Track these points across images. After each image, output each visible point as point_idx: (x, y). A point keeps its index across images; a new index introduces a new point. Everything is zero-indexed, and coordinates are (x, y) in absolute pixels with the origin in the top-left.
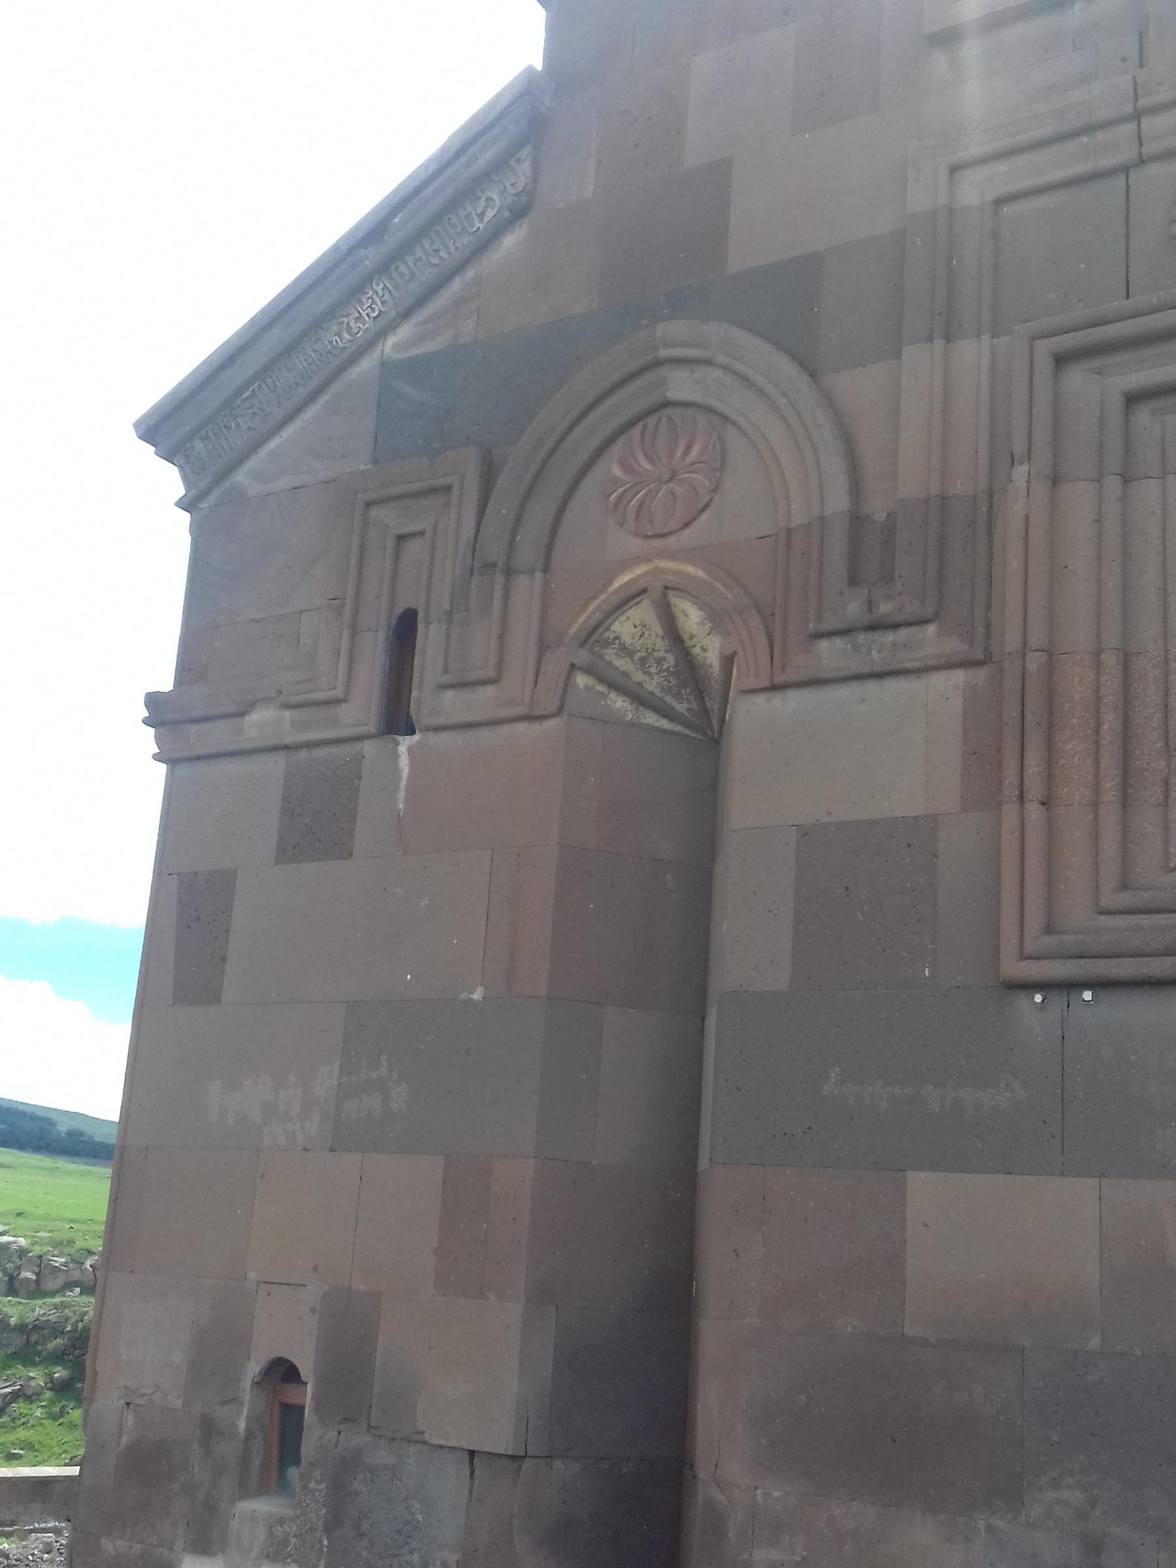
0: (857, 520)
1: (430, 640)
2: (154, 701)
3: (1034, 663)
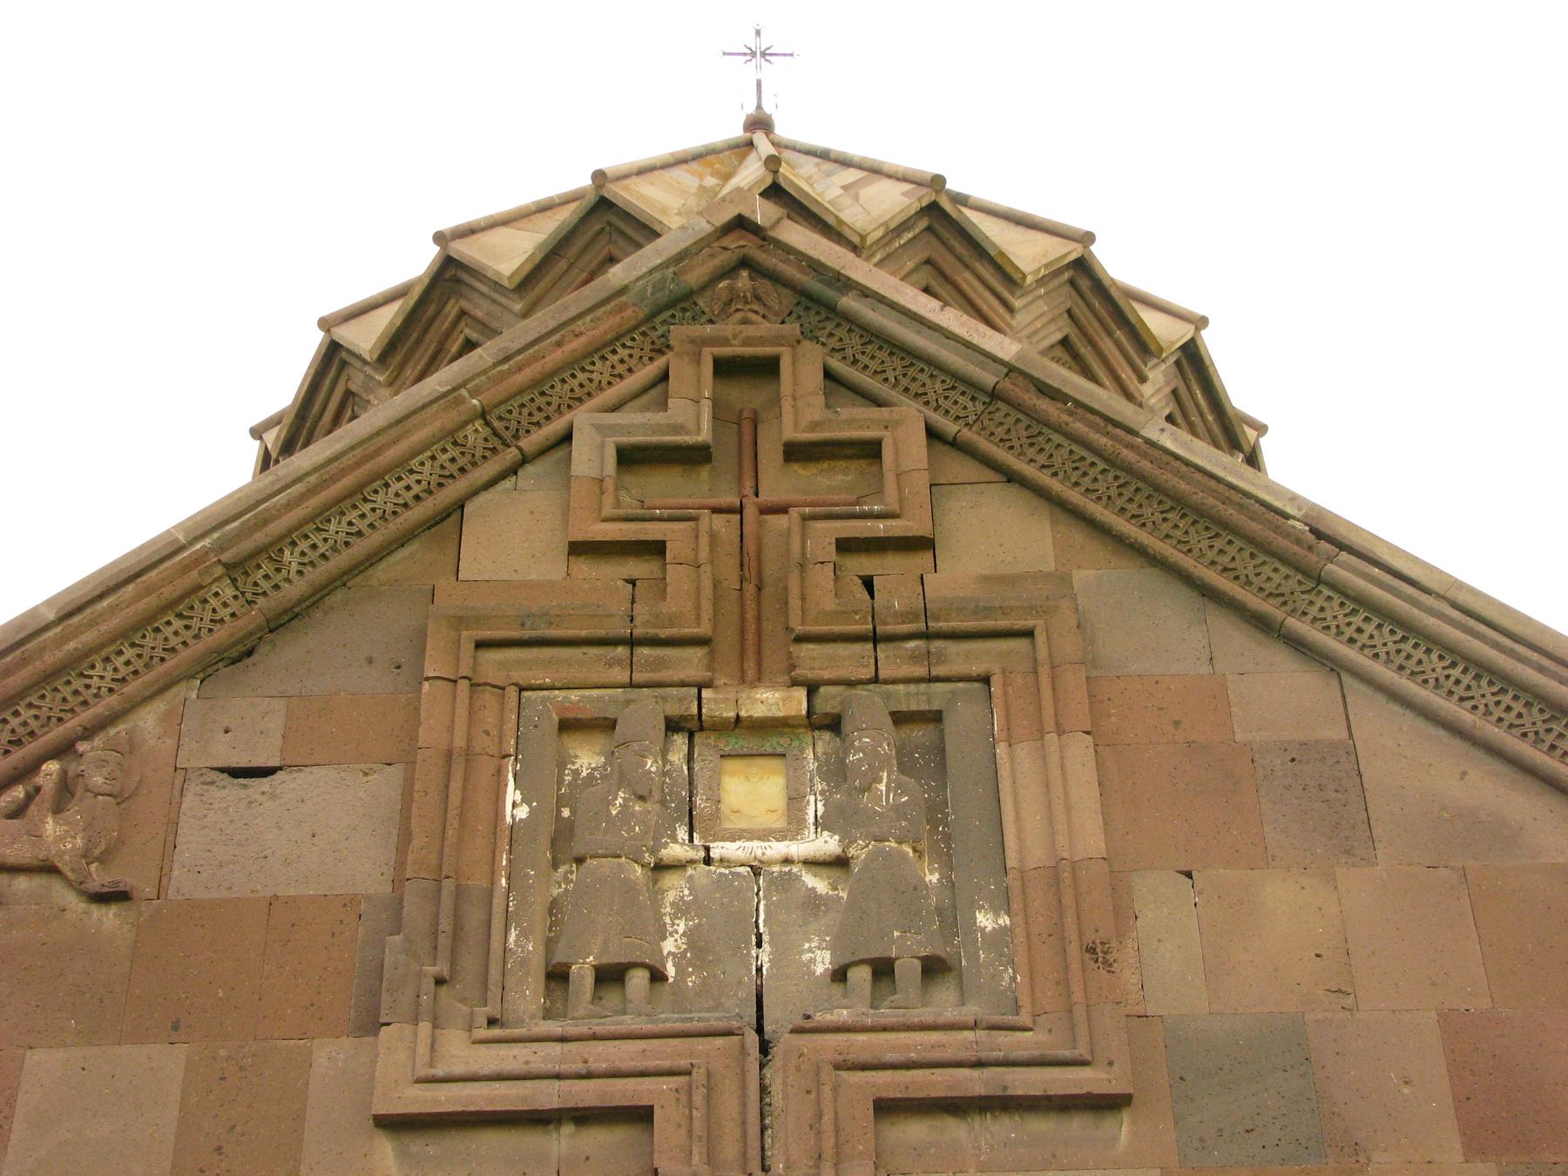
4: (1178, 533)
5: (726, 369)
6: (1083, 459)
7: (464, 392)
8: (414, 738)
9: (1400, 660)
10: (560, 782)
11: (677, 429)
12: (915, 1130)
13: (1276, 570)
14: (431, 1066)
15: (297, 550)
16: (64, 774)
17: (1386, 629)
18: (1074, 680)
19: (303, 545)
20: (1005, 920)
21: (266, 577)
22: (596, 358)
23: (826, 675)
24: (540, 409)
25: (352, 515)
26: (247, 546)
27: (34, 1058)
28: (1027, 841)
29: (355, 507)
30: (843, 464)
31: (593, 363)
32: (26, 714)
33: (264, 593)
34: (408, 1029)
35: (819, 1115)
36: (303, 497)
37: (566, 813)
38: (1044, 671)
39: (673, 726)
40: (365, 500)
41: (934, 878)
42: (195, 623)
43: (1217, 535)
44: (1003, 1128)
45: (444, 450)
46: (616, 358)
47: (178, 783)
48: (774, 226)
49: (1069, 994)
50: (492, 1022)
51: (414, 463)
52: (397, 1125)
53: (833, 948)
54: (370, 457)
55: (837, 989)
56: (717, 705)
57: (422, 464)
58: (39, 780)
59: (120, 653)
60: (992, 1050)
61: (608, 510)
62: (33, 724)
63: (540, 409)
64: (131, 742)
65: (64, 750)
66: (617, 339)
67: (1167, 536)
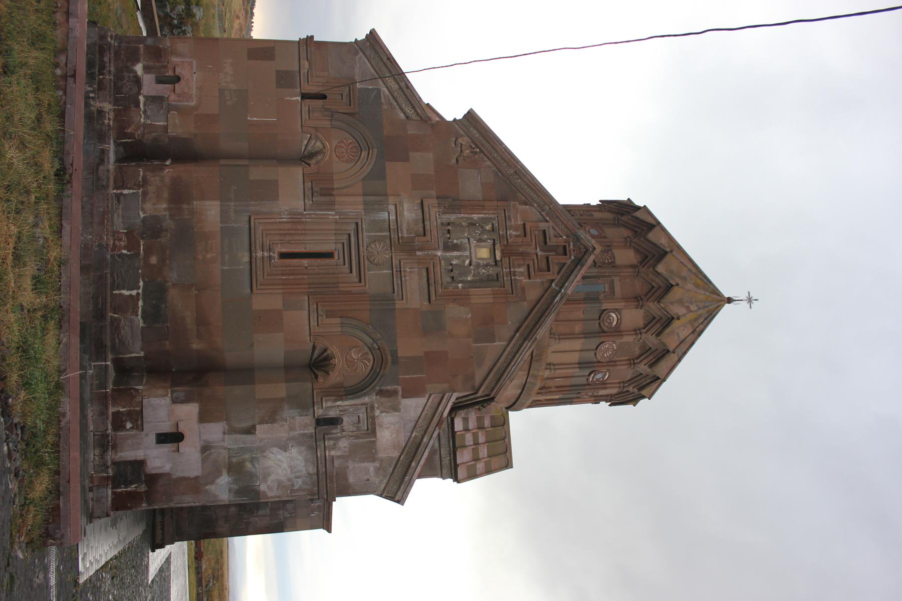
0: (333, 189)
1: (320, 103)
2: (312, 37)
3: (304, 220)
5: (565, 247)
12: (425, 274)
28: (472, 291)
44: (426, 286)
56: (498, 246)
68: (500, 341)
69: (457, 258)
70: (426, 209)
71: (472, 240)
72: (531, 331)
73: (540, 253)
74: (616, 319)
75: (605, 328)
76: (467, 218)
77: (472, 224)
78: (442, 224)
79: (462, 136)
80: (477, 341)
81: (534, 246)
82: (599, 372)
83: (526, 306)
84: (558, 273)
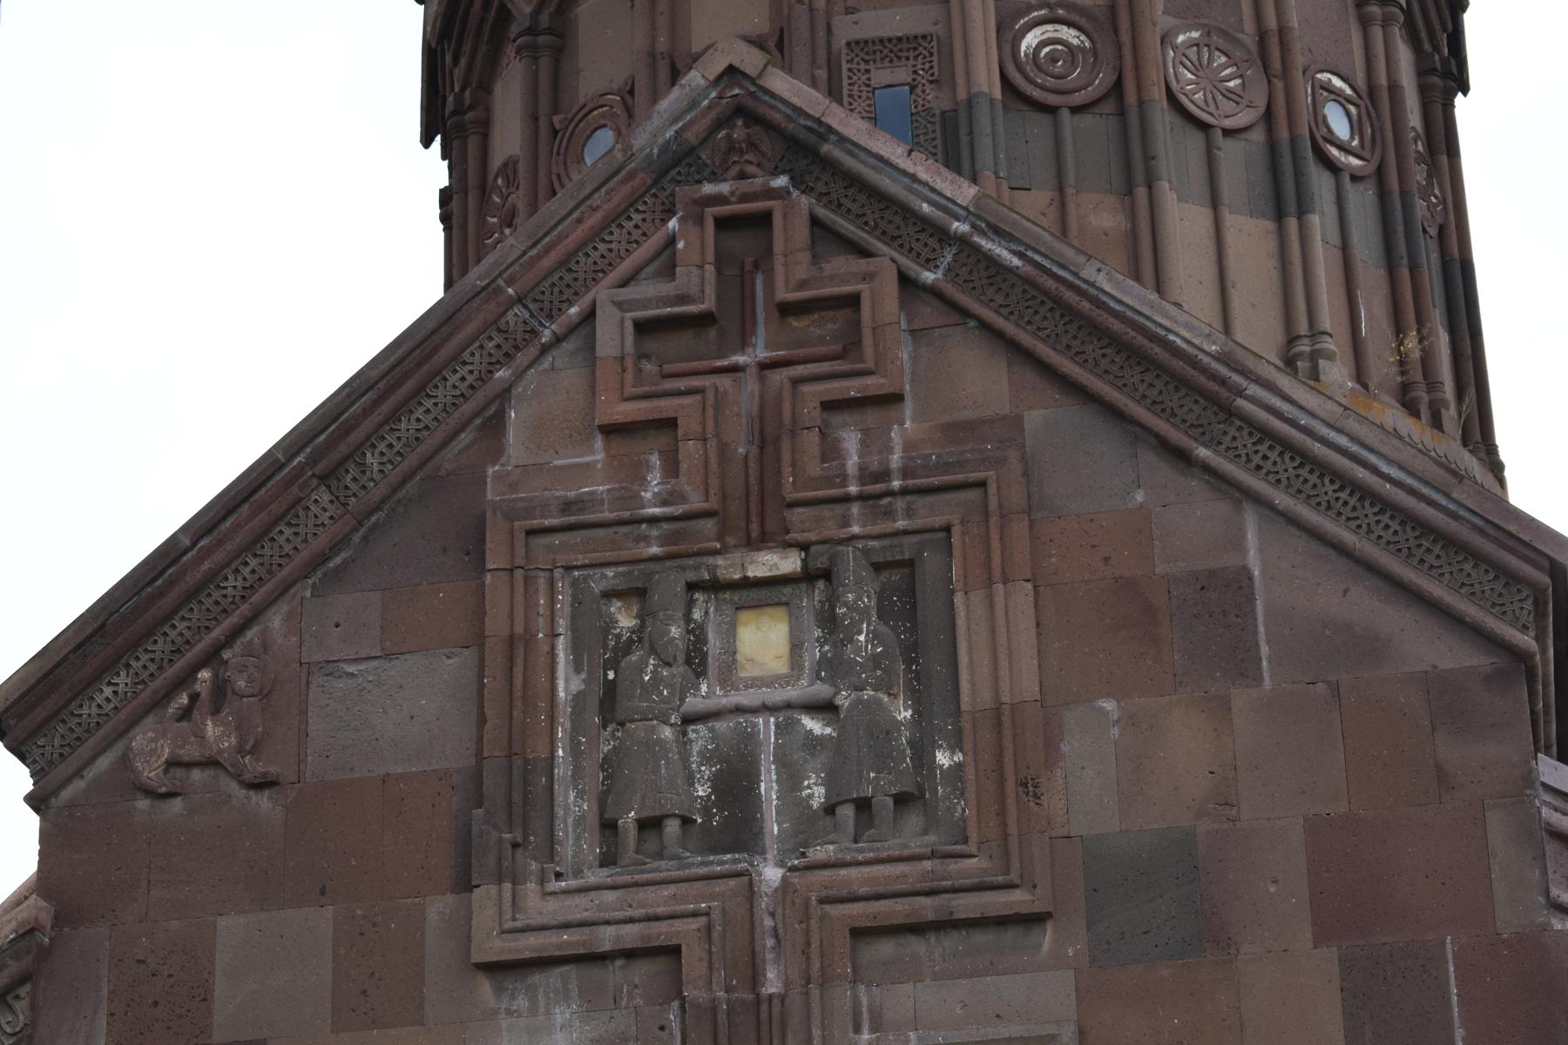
4: (1114, 368)
5: (722, 224)
6: (1034, 297)
7: (500, 282)
8: (482, 629)
9: (1298, 484)
10: (605, 647)
11: (683, 299)
12: (885, 948)
13: (1196, 402)
14: (514, 919)
15: (377, 451)
16: (216, 676)
17: (1287, 456)
18: (1019, 528)
19: (382, 447)
20: (958, 757)
21: (355, 479)
22: (614, 228)
23: (813, 536)
24: (568, 286)
25: (419, 413)
26: (335, 456)
27: (223, 923)
28: (973, 689)
29: (420, 404)
30: (831, 313)
31: (611, 233)
32: (181, 626)
33: (355, 495)
34: (493, 889)
35: (808, 943)
36: (377, 403)
37: (611, 675)
38: (994, 520)
39: (692, 587)
40: (428, 396)
41: (909, 714)
42: (301, 529)
43: (1147, 370)
44: (951, 941)
45: (490, 338)
46: (631, 224)
47: (304, 676)
48: (760, 75)
49: (1006, 825)
50: (558, 876)
51: (466, 356)
52: (493, 969)
53: (830, 783)
54: (428, 357)
55: (828, 820)
56: (728, 567)
57: (473, 354)
58: (197, 687)
59: (246, 564)
60: (944, 879)
61: (630, 390)
62: (188, 634)
63: (568, 286)
64: (265, 646)
65: (211, 658)
66: (631, 205)
67: (1106, 372)
68: (1239, 545)
69: (791, 780)
70: (529, 945)
71: (693, 703)
72: (1180, 382)
73: (762, 354)
74: (1049, 31)
75: (1101, 81)
76: (576, 729)
77: (609, 703)
78: (607, 860)
79: (125, 761)
80: (1247, 671)
81: (725, 382)
82: (1320, 120)
83: (1043, 415)
84: (865, 253)
